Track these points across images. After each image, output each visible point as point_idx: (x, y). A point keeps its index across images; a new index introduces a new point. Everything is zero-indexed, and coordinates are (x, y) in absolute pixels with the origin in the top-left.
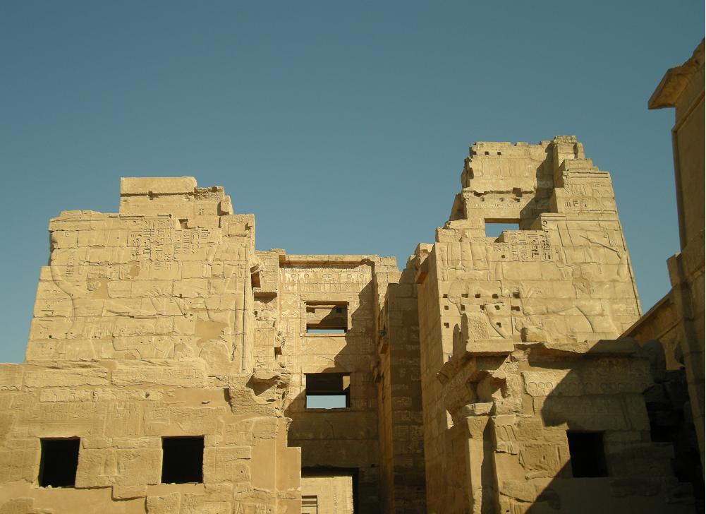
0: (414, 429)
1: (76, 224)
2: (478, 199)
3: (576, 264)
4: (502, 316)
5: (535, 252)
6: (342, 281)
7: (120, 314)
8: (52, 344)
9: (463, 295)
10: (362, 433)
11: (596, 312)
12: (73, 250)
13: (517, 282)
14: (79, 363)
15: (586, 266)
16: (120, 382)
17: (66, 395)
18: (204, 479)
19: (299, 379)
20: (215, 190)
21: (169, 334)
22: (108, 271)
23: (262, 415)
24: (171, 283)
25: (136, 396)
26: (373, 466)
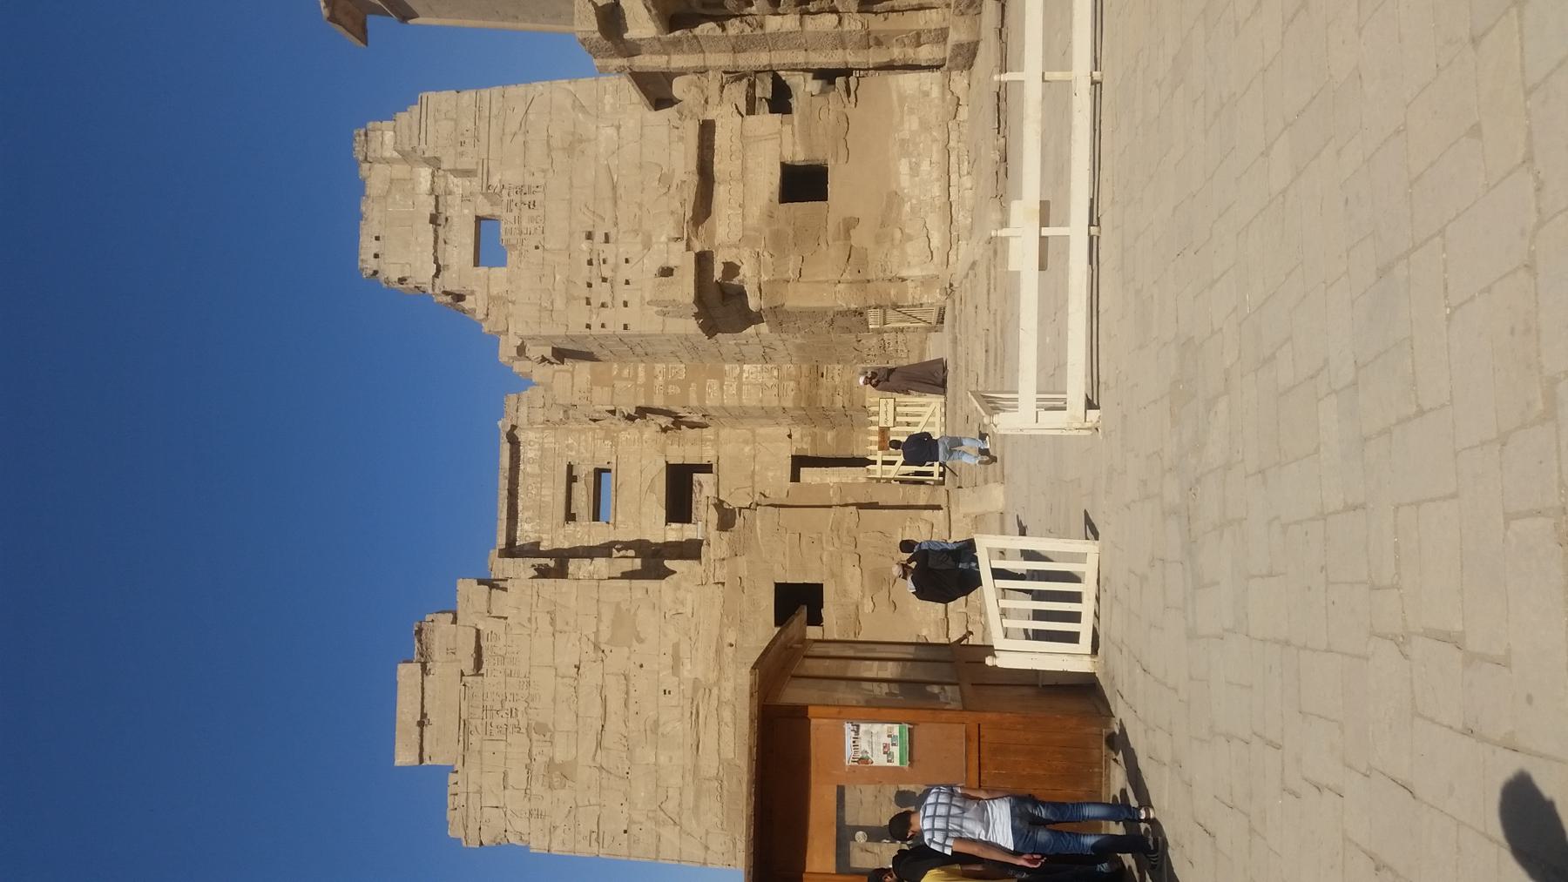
0: (746, 378)
1: (471, 810)
2: (444, 274)
4: (616, 257)
7: (599, 744)
8: (634, 829)
9: (588, 303)
10: (747, 449)
11: (615, 134)
12: (509, 812)
13: (571, 234)
15: (553, 142)
19: (674, 533)
20: (420, 632)
22: (541, 760)
23: (755, 520)
24: (559, 679)
25: (731, 655)
26: (790, 436)
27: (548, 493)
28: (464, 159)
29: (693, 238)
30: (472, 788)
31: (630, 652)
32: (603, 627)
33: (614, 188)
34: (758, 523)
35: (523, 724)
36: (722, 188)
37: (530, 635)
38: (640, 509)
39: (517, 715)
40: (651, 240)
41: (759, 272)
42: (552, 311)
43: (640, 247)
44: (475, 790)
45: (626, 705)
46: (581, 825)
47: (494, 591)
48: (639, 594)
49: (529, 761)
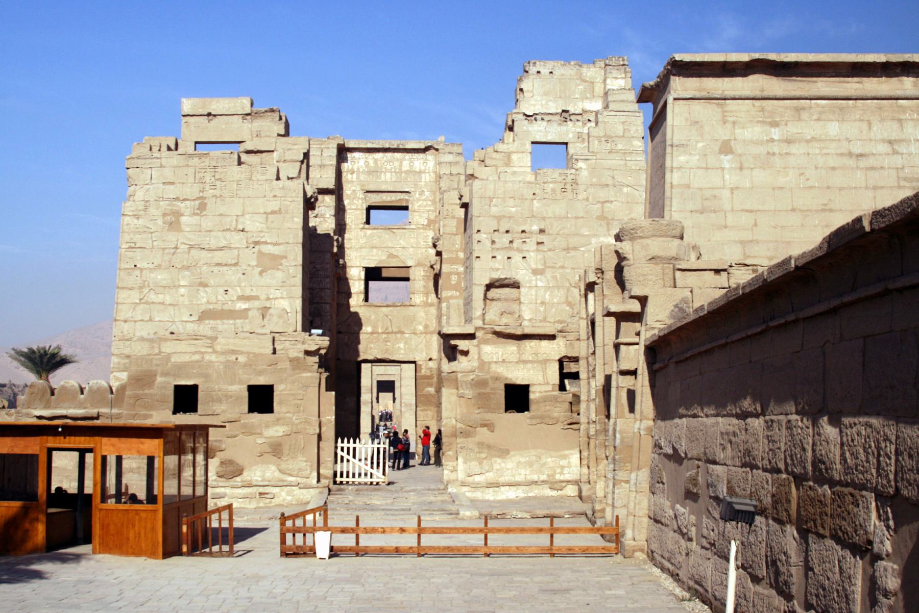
3: (599, 202)
4: (528, 251)
5: (564, 190)
6: (404, 169)
7: (191, 247)
8: (137, 272)
10: (421, 328)
12: (148, 187)
13: (544, 219)
15: (608, 205)
17: (186, 358)
18: (275, 411)
19: (358, 273)
21: (236, 264)
24: (235, 218)
25: (230, 359)
26: (430, 359)
28: (596, 143)
30: (164, 161)
31: (253, 266)
32: (270, 247)
33: (575, 249)
34: (309, 374)
35: (205, 194)
38: (376, 248)
40: (539, 274)
41: (463, 372)
43: (534, 266)
45: (218, 264)
47: (299, 164)
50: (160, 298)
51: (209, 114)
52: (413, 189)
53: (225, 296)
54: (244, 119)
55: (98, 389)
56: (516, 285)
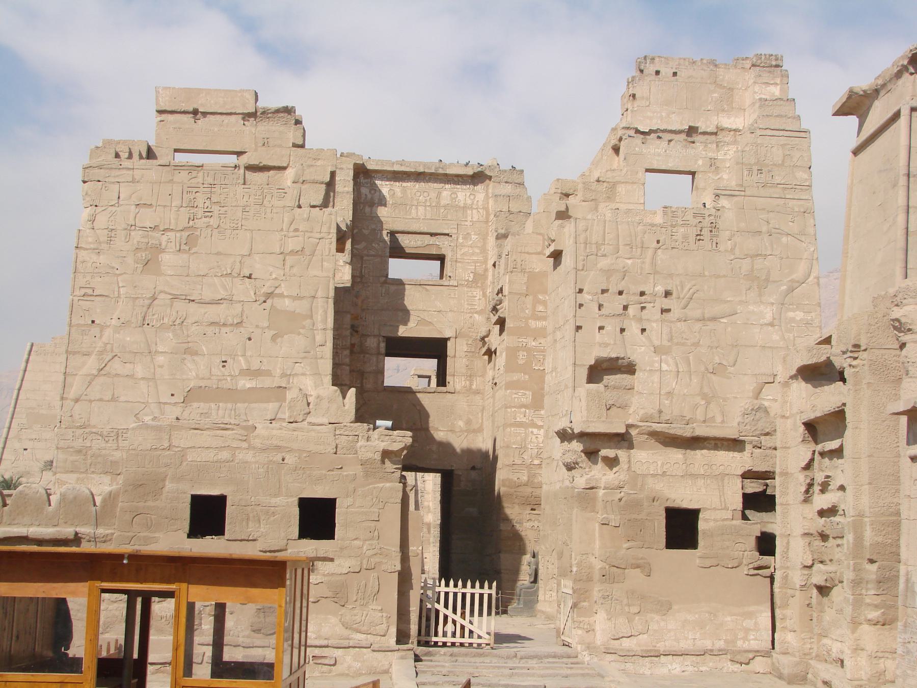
0: (532, 432)
5: (699, 237)
6: (443, 202)
7: (175, 297)
8: (95, 330)
9: (604, 291)
10: (461, 423)
11: (765, 321)
12: (114, 209)
13: (671, 276)
14: (219, 425)
16: (260, 446)
17: (210, 456)
18: (336, 537)
19: (375, 345)
21: (240, 324)
23: (391, 482)
24: (238, 259)
25: (275, 459)
26: (473, 468)
27: (419, 214)
29: (638, 430)
30: (138, 174)
31: (263, 328)
33: (714, 319)
34: (388, 485)
36: (680, 456)
37: (282, 230)
39: (205, 217)
40: (664, 354)
42: (597, 255)
43: (657, 343)
44: (135, 177)
45: (213, 323)
46: (100, 279)
47: (324, 186)
48: (319, 338)
49: (162, 229)
50: (127, 369)
51: (195, 112)
52: (455, 231)
53: (223, 369)
54: (244, 119)
55: (75, 498)
56: (630, 369)
